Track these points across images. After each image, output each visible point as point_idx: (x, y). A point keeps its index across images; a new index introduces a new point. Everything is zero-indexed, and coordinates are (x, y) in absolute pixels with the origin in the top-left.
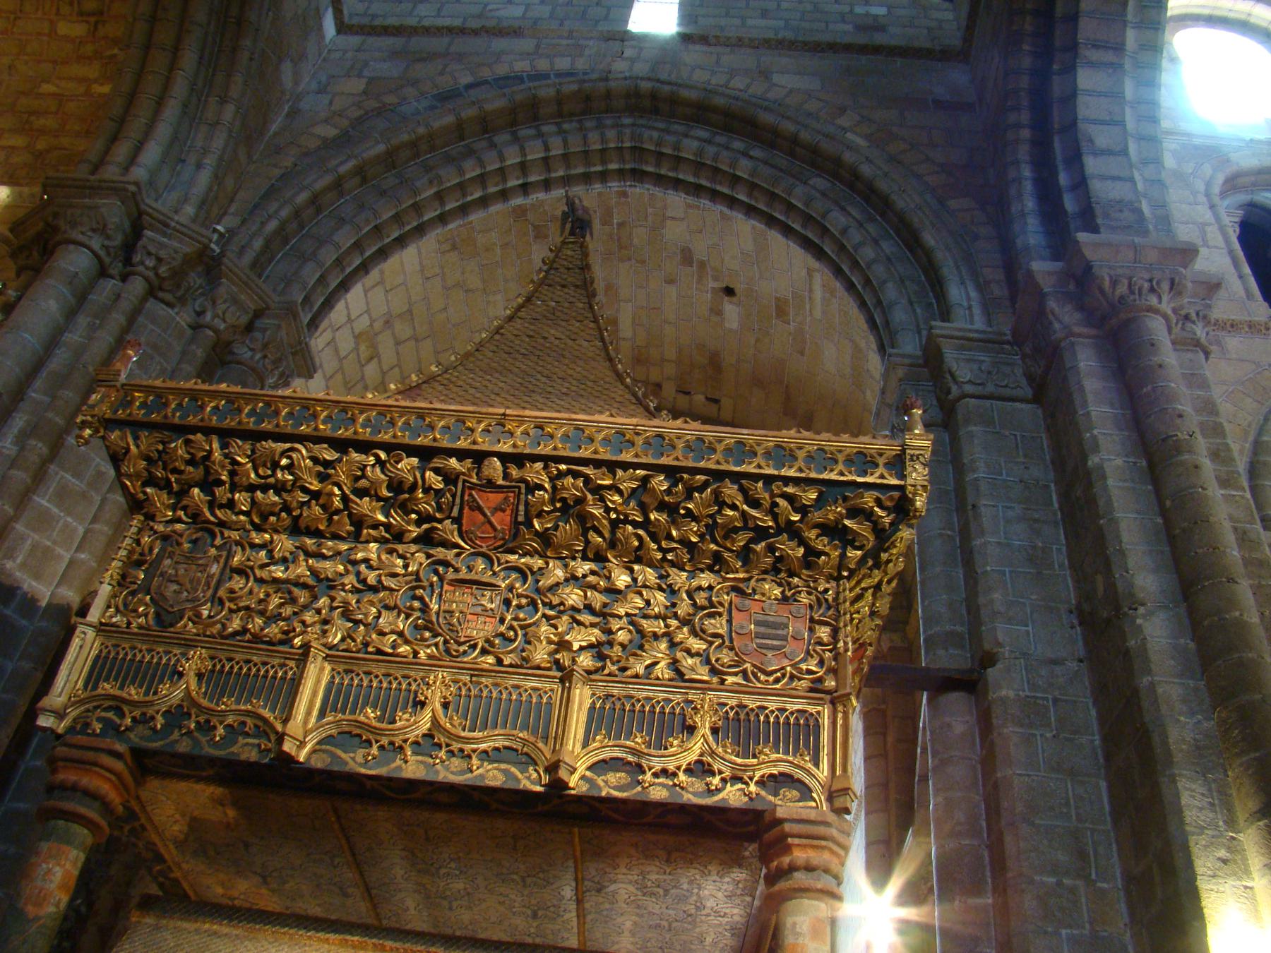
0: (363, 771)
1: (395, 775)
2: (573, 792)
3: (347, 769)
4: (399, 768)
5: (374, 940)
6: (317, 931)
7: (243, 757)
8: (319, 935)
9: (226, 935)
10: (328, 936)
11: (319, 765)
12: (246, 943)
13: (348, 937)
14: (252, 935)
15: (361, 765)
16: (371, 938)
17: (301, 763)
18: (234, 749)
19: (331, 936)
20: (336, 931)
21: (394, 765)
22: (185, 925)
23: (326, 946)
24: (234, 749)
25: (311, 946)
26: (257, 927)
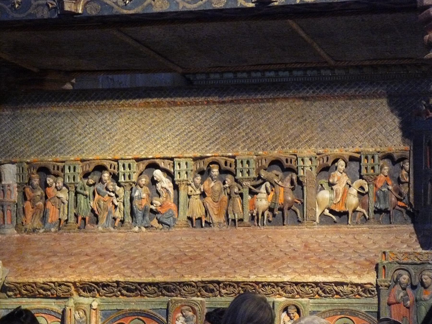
0: (125, 12)
1: (149, 11)
2: (276, 4)
3: (114, 12)
4: (150, 4)
5: (168, 99)
6: (127, 98)
7: (39, 16)
8: (128, 102)
9: (64, 113)
10: (135, 101)
11: (94, 13)
12: (80, 117)
13: (149, 100)
14: (82, 110)
15: (122, 7)
16: (165, 97)
17: (80, 14)
18: (31, 11)
19: (138, 101)
20: (139, 97)
21: (145, 4)
22: (34, 111)
23: (135, 109)
24: (31, 11)
25: (125, 110)
26: (84, 103)
